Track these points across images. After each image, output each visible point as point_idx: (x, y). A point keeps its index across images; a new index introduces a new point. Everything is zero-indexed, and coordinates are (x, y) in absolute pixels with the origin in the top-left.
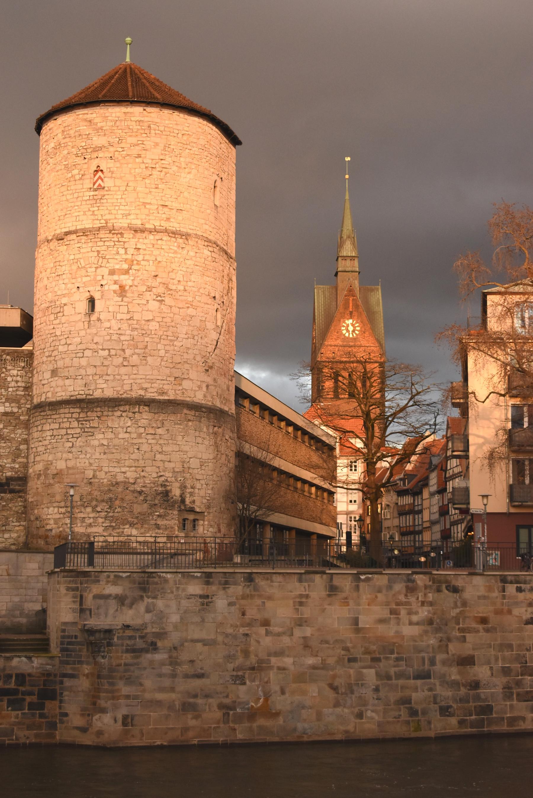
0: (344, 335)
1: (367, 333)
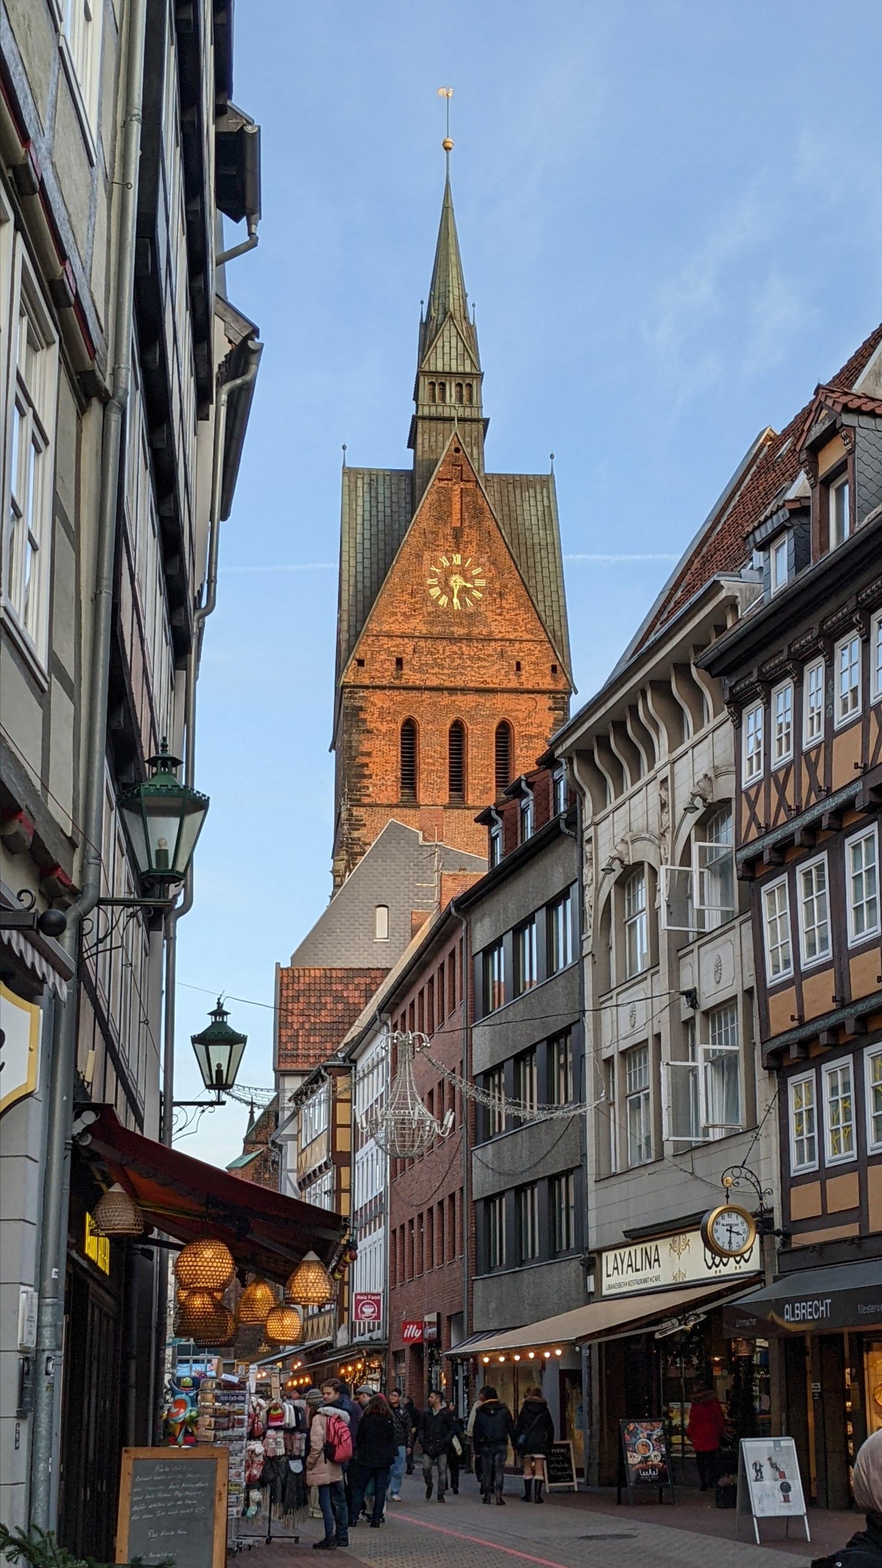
0: (435, 603)
1: (511, 598)
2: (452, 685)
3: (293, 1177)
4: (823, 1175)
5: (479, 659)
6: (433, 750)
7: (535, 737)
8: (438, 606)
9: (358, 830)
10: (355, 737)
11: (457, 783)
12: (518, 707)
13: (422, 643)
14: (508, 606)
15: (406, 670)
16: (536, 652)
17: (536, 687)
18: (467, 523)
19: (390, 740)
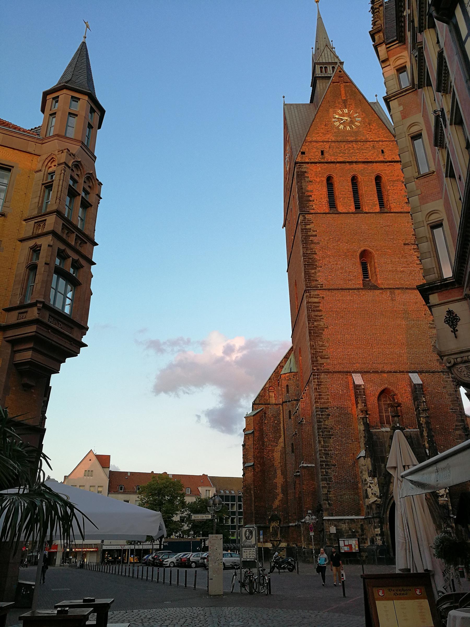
2: (350, 160)
5: (362, 149)
6: (343, 189)
7: (396, 181)
8: (339, 129)
9: (309, 225)
10: (304, 184)
12: (385, 169)
13: (333, 144)
14: (373, 128)
15: (326, 155)
16: (391, 145)
17: (393, 160)
18: (348, 97)
19: (322, 185)
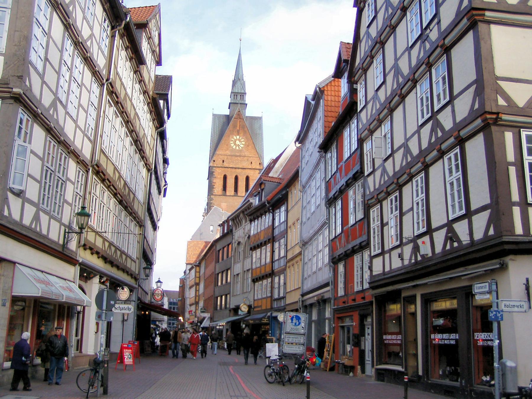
3: (188, 287)
4: (258, 299)
6: (231, 182)
11: (236, 190)
